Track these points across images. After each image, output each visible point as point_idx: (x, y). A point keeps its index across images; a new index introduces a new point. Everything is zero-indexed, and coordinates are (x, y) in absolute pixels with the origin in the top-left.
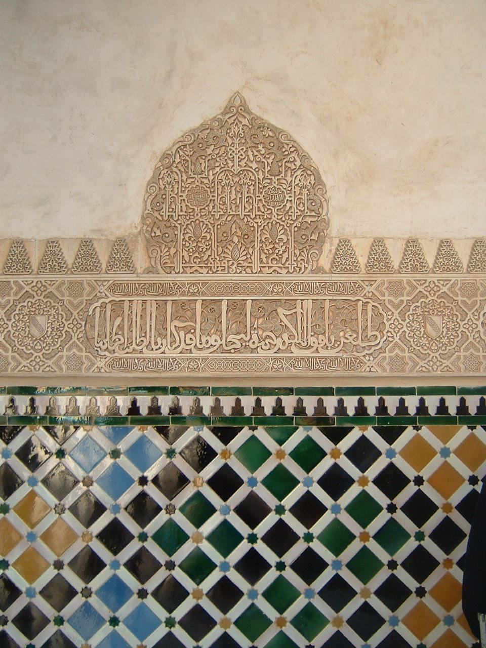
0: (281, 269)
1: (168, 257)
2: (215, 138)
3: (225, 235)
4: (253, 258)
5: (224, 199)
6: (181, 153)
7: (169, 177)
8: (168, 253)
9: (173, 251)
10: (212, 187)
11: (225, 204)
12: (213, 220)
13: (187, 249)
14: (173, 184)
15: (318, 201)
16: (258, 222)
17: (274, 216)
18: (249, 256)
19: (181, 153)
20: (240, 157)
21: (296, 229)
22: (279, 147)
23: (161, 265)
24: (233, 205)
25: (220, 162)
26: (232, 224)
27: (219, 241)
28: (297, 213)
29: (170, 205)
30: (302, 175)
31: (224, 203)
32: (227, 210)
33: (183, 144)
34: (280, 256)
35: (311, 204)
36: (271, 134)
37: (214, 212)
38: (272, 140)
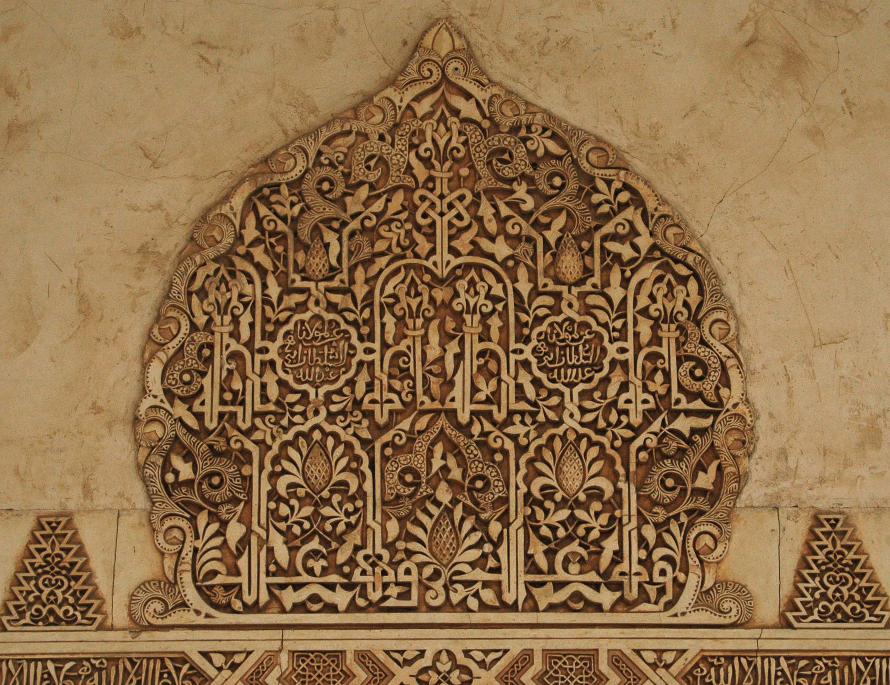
1: (217, 554)
2: (372, 163)
3: (409, 478)
4: (502, 551)
6: (263, 210)
7: (223, 288)
8: (218, 541)
9: (235, 532)
10: (365, 322)
12: (368, 428)
13: (282, 526)
14: (237, 312)
15: (714, 363)
16: (518, 435)
17: (572, 415)
18: (488, 548)
19: (263, 210)
20: (456, 222)
21: (643, 455)
22: (581, 189)
23: (195, 580)
24: (433, 379)
25: (393, 235)
26: (434, 443)
28: (645, 401)
29: (225, 381)
30: (659, 279)
31: (405, 374)
32: (414, 394)
33: (268, 182)
34: (592, 548)
35: (692, 373)
37: (373, 401)
38: (559, 167)
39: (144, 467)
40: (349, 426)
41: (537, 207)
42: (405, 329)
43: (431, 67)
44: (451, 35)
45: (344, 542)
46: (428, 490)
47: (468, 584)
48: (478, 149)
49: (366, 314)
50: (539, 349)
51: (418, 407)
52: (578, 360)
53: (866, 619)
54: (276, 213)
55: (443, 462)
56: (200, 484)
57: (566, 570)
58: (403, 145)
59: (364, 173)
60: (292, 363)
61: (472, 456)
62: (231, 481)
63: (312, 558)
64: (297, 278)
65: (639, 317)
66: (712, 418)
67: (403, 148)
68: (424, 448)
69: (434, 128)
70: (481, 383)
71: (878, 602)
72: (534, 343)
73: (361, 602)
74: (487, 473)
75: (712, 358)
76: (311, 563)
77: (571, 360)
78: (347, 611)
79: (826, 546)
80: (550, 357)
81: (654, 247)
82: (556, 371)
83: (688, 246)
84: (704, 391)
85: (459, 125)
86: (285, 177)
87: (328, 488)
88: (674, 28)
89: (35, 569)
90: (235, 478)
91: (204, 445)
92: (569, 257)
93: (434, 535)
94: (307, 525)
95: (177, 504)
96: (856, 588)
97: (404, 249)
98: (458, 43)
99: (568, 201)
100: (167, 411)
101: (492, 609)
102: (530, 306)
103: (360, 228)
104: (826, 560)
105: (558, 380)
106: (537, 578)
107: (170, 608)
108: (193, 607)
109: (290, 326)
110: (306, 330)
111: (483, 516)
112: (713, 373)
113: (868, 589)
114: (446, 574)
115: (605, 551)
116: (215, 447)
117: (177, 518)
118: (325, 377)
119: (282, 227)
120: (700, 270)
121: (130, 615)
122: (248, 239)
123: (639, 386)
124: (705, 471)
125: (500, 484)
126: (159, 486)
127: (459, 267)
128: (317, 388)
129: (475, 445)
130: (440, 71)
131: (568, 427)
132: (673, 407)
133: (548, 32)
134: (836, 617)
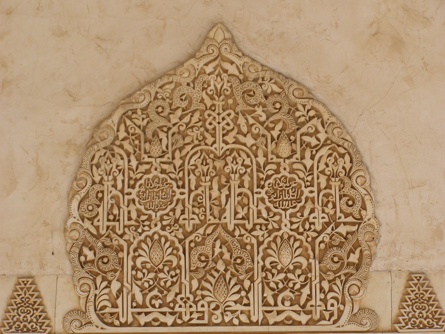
0: (299, 314)
1: (106, 297)
2: (183, 98)
3: (203, 258)
4: (250, 295)
5: (198, 198)
6: (128, 122)
7: (108, 162)
9: (115, 286)
10: (180, 179)
11: (203, 206)
13: (139, 283)
14: (115, 174)
15: (358, 199)
16: (258, 236)
17: (286, 226)
18: (243, 293)
19: (128, 122)
20: (226, 127)
21: (323, 246)
22: (290, 110)
23: (96, 310)
25: (194, 134)
26: (215, 241)
27: (192, 268)
28: (323, 218)
29: (110, 210)
30: (330, 155)
32: (205, 215)
33: (131, 108)
36: (276, 89)
37: (184, 219)
38: (279, 99)
39: (69, 253)
40: (172, 232)
41: (267, 119)
42: (201, 182)
43: (213, 48)
44: (223, 32)
45: (170, 291)
46: (213, 264)
47: (233, 312)
48: (237, 90)
49: (181, 174)
50: (269, 191)
51: (208, 222)
52: (289, 197)
53: (434, 327)
54: (135, 124)
55: (220, 250)
56: (98, 262)
57: (283, 304)
58: (199, 88)
59: (179, 103)
60: (143, 200)
61: (235, 247)
62: (113, 260)
63: (154, 299)
64: (146, 156)
65: (320, 175)
66: (357, 226)
67: (199, 90)
68: (210, 242)
69: (215, 79)
70: (239, 209)
71: (441, 318)
72: (266, 188)
73: (179, 322)
74: (242, 255)
75: (357, 195)
76: (154, 302)
77: (285, 197)
78: (173, 325)
79: (415, 291)
80: (274, 195)
81: (327, 139)
82: (278, 202)
83: (345, 138)
84: (353, 212)
85: (227, 77)
86: (139, 105)
87: (162, 263)
88: (337, 27)
89: (17, 305)
90: (115, 259)
91: (100, 242)
92: (284, 144)
93: (216, 287)
94: (151, 283)
95: (86, 272)
96: (430, 312)
97: (200, 141)
98: (227, 35)
99: (283, 116)
100: (81, 225)
101: (246, 324)
102: (264, 169)
103: (178, 130)
104: (415, 298)
105: (278, 207)
106: (269, 309)
107: (83, 324)
108: (94, 324)
109: (142, 181)
110: (151, 183)
111: (241, 277)
112: (357, 203)
113: (436, 312)
114: (222, 307)
115: (303, 295)
116: (105, 243)
117: (86, 279)
118: (160, 207)
119: (138, 131)
120: (351, 151)
121: (63, 327)
122: (121, 137)
123: (320, 210)
124: (354, 253)
125: (250, 261)
126: (77, 263)
127: (228, 150)
128: (156, 212)
129: (236, 241)
130: (218, 51)
131: (284, 231)
132: (338, 221)
133: (273, 29)
134: (420, 326)
